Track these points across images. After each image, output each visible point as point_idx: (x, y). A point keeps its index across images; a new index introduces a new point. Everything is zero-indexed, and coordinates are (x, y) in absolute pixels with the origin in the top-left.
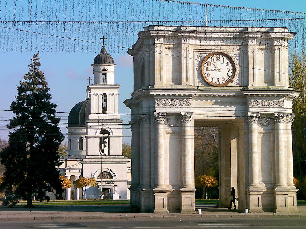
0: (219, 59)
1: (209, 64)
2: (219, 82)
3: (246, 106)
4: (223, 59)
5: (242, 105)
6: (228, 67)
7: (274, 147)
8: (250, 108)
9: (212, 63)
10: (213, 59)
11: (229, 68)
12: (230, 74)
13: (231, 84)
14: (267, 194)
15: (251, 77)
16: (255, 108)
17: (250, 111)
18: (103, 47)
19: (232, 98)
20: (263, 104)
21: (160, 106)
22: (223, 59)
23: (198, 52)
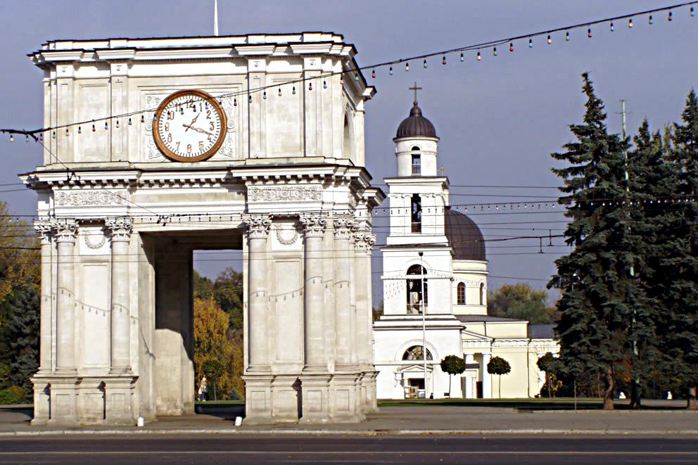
8: (251, 204)
9: (175, 113)
11: (212, 123)
13: (217, 156)
16: (261, 203)
18: (415, 104)
21: (65, 206)
23: (148, 92)
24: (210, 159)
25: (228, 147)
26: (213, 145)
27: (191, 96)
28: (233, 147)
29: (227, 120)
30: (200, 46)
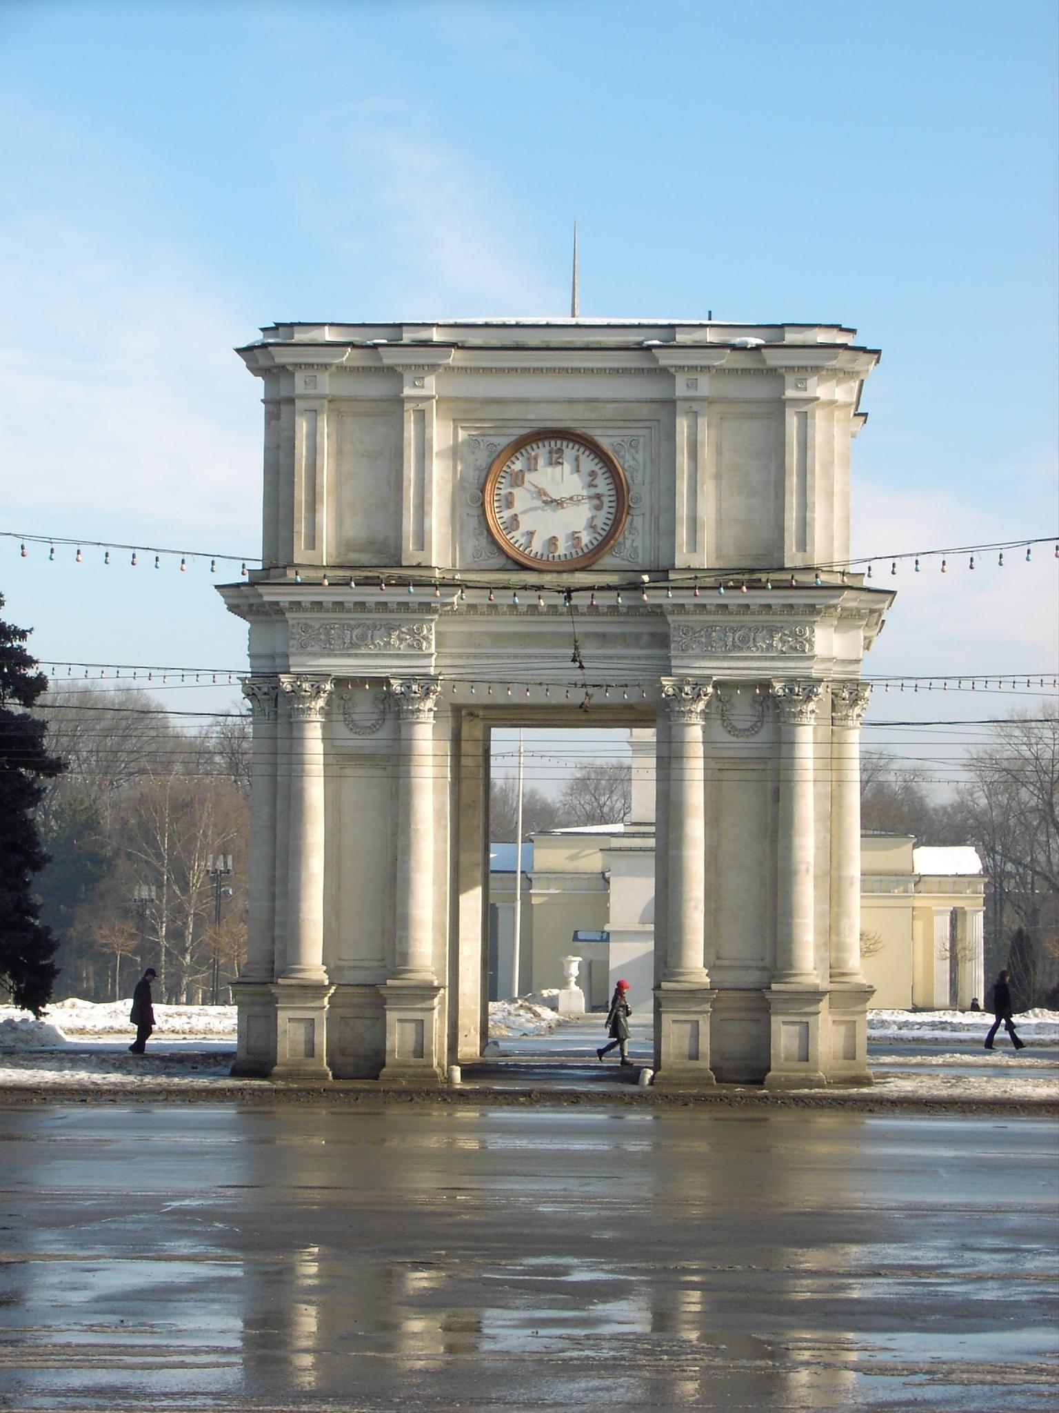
0: (560, 460)
1: (517, 479)
2: (556, 554)
3: (662, 652)
4: (577, 459)
5: (649, 647)
6: (600, 490)
7: (775, 819)
8: (676, 657)
10: (536, 459)
12: (602, 518)
13: (608, 561)
14: (739, 1009)
15: (682, 533)
17: (674, 671)
19: (622, 619)
20: (730, 643)
22: (577, 459)
24: (594, 567)
25: (628, 543)
26: (600, 538)
27: (559, 442)
28: (638, 543)
29: (629, 491)
30: (578, 345)
